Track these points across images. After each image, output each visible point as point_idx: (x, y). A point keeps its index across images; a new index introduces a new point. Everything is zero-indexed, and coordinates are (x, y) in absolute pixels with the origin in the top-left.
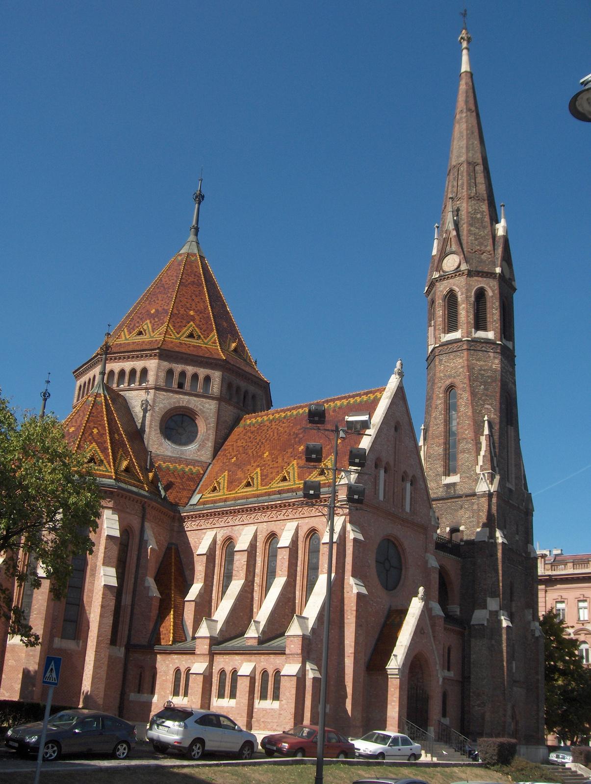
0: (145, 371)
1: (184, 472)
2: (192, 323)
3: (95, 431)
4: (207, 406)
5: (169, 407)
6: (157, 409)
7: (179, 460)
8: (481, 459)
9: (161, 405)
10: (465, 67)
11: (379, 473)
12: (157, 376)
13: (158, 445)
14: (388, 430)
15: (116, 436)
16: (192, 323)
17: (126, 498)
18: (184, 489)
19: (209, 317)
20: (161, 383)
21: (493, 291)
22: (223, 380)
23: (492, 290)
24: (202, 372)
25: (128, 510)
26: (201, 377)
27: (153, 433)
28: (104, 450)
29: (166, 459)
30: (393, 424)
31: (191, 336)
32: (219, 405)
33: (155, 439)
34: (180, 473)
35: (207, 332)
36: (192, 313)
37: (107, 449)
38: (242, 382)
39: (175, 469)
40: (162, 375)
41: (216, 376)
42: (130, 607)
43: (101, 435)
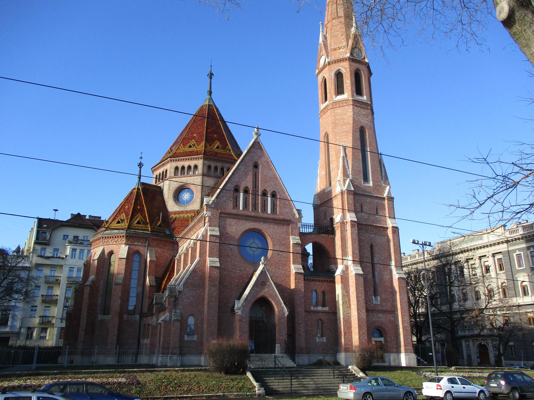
1: (184, 218)
2: (193, 140)
3: (127, 207)
4: (196, 180)
6: (171, 188)
7: (182, 212)
8: (339, 171)
9: (173, 186)
11: (240, 194)
12: (170, 172)
13: (171, 206)
14: (245, 168)
15: (139, 207)
16: (193, 140)
17: (133, 237)
19: (203, 135)
21: (345, 69)
25: (136, 243)
26: (192, 166)
27: (170, 201)
29: (175, 213)
30: (251, 164)
31: (190, 147)
34: (182, 218)
35: (199, 143)
36: (195, 135)
37: (128, 215)
40: (173, 170)
41: (200, 163)
42: (141, 295)
43: (129, 208)
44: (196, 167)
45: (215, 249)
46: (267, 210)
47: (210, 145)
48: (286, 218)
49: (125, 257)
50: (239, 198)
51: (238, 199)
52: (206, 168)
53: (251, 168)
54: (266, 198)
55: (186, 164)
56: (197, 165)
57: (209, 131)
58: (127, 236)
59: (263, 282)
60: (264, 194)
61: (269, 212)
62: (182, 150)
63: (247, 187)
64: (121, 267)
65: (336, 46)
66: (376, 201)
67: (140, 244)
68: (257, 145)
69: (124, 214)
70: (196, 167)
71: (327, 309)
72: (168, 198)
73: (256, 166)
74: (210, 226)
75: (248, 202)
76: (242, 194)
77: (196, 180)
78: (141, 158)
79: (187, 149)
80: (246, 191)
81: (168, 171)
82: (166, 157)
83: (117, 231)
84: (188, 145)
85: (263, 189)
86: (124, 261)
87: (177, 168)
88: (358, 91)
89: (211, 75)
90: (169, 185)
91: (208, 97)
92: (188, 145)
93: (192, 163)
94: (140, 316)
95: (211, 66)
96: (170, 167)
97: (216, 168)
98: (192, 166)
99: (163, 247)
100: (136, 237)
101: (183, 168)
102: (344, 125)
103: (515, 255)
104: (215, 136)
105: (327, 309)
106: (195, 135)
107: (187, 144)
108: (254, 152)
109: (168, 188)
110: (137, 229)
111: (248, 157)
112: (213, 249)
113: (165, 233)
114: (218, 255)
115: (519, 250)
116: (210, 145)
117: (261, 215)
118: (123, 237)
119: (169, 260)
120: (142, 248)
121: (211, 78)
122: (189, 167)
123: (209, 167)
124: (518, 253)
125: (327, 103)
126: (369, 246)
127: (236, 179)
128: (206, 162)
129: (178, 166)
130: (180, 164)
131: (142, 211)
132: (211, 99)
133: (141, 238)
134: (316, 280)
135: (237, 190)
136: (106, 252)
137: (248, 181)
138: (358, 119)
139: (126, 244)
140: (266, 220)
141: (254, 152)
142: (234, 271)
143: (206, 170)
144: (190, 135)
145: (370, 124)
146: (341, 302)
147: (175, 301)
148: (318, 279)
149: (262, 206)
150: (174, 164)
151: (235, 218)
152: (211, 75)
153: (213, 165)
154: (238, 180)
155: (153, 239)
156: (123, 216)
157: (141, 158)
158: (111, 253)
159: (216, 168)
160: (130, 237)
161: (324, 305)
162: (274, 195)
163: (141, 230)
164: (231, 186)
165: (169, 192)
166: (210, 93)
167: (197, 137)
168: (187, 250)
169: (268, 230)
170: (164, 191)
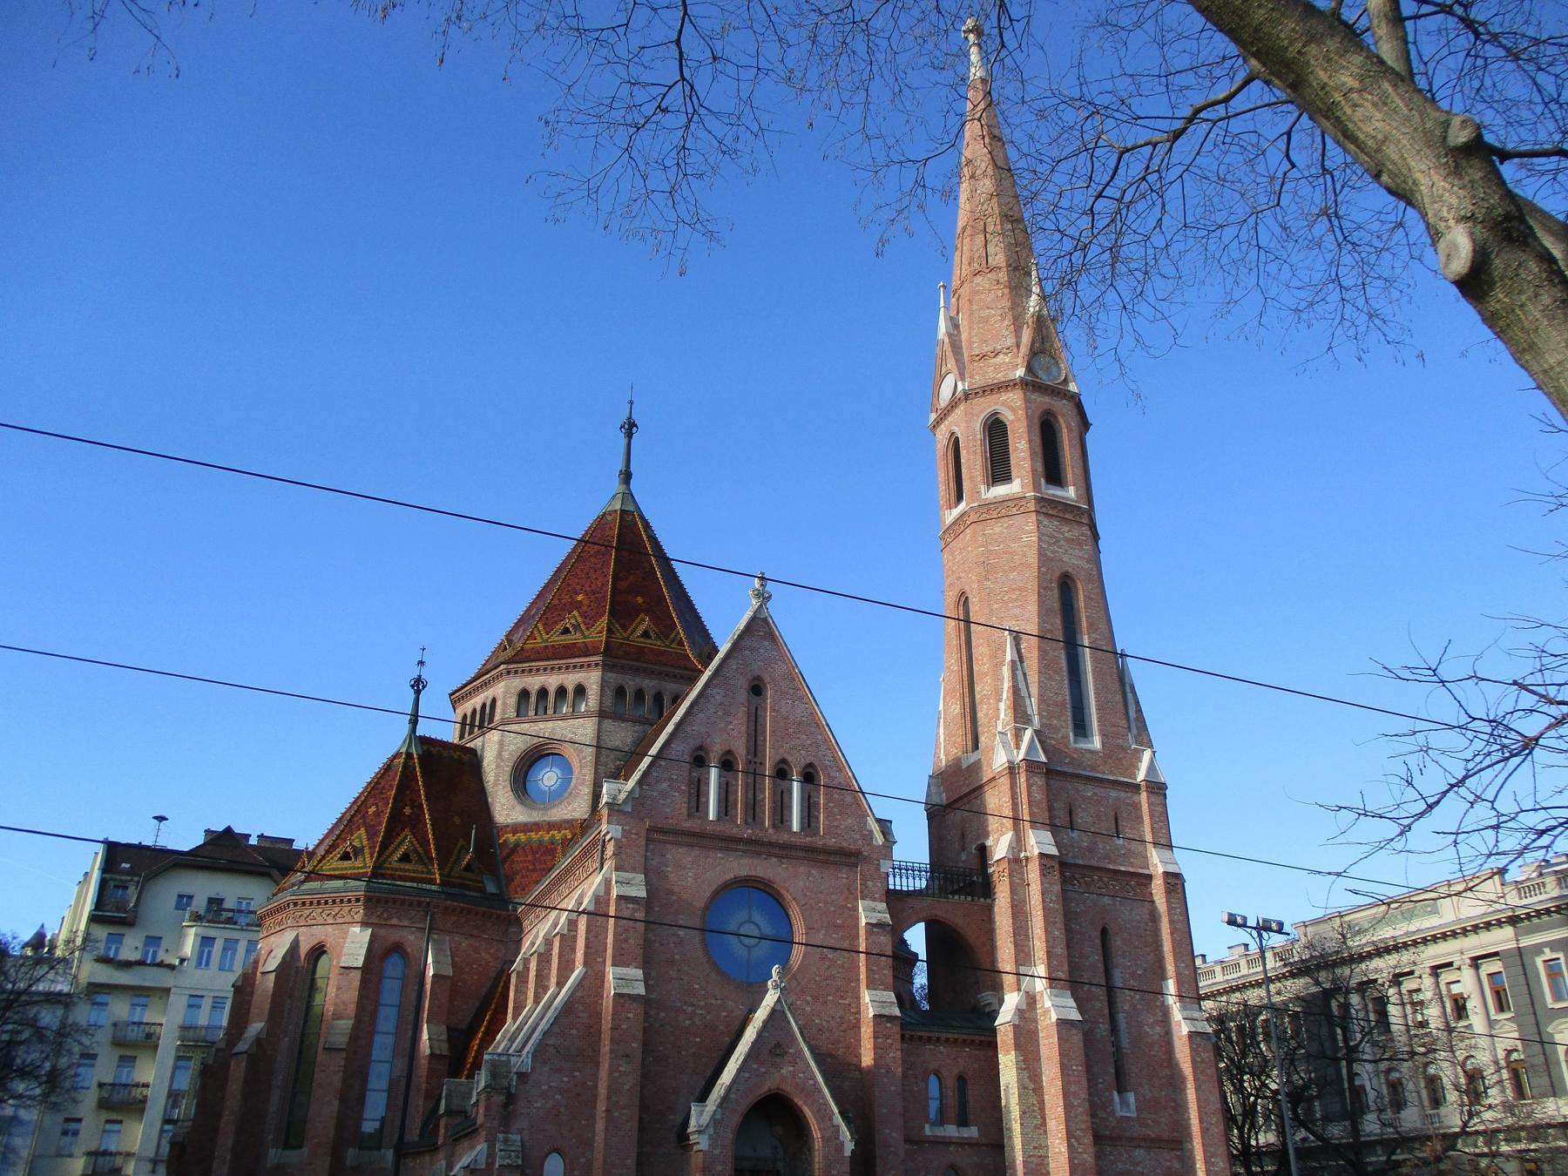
0: (494, 701)
1: (540, 842)
2: (575, 613)
3: (373, 809)
4: (581, 731)
5: (523, 747)
6: (506, 755)
7: (536, 827)
8: (1002, 706)
10: (976, 72)
12: (504, 704)
13: (505, 809)
15: (407, 811)
16: (575, 613)
17: (386, 902)
18: (534, 870)
19: (604, 597)
20: (512, 714)
21: (1014, 410)
22: (604, 684)
23: (1013, 409)
24: (570, 680)
25: (394, 921)
26: (570, 688)
27: (501, 793)
28: (371, 836)
29: (516, 828)
30: (742, 684)
31: (566, 631)
32: (600, 723)
33: (503, 801)
34: (535, 845)
35: (590, 620)
36: (580, 597)
37: (376, 834)
38: (647, 681)
39: (529, 841)
40: (513, 701)
41: (592, 679)
43: (378, 814)
44: (580, 691)
45: (631, 941)
46: (790, 821)
47: (625, 628)
48: (845, 844)
49: (360, 963)
50: (707, 785)
51: (703, 787)
52: (609, 693)
53: (743, 695)
54: (785, 784)
55: (552, 681)
56: (585, 684)
57: (622, 585)
58: (368, 900)
59: (778, 1045)
60: (782, 773)
61: (795, 827)
62: (542, 639)
63: (729, 752)
64: (345, 997)
65: (987, 348)
66: (1113, 794)
67: (406, 923)
68: (759, 629)
69: (363, 830)
70: (580, 691)
71: (972, 1132)
72: (496, 784)
73: (757, 689)
74: (617, 869)
75: (731, 798)
76: (714, 773)
77: (581, 731)
78: (421, 663)
79: (556, 639)
80: (727, 765)
81: (499, 703)
82: (494, 662)
83: (339, 883)
84: (560, 627)
85: (778, 758)
86: (356, 977)
87: (524, 694)
88: (1052, 472)
89: (630, 428)
90: (501, 743)
91: (622, 488)
92: (560, 627)
93: (570, 680)
94: (396, 1151)
95: (631, 403)
96: (503, 691)
97: (639, 695)
98: (570, 688)
99: (475, 932)
100: (395, 901)
101: (543, 693)
102: (1013, 569)
103: (1539, 961)
104: (640, 600)
105: (972, 1132)
106: (580, 597)
107: (556, 623)
108: (752, 649)
109: (496, 753)
110: (401, 878)
111: (733, 664)
112: (626, 941)
113: (482, 890)
114: (640, 959)
115: (1554, 946)
116: (625, 628)
117: (772, 835)
118: (358, 900)
119: (493, 975)
120: (412, 938)
121: (629, 435)
122: (561, 691)
123: (620, 692)
124: (1548, 954)
125: (962, 506)
126: (1098, 934)
127: (697, 727)
128: (611, 676)
129: (530, 688)
130: (534, 683)
131: (416, 823)
132: (628, 496)
133: (411, 904)
134: (938, 1039)
135: (700, 761)
136: (304, 949)
137: (735, 733)
138: (1054, 552)
139: (364, 924)
140: (786, 851)
141: (752, 649)
142: (690, 1009)
143: (609, 702)
144: (566, 599)
145: (1087, 566)
146: (1019, 1158)
147: (506, 1105)
148: (943, 1036)
149: (774, 809)
150: (517, 683)
151: (692, 846)
152: (630, 428)
153: (631, 683)
154: (703, 730)
155: (447, 908)
156: (360, 837)
157: (421, 663)
158: (319, 951)
159: (639, 695)
160: (379, 901)
161: (963, 1122)
162: (809, 777)
163: (413, 880)
164: (682, 749)
165: (498, 766)
166: (627, 476)
167: (586, 602)
168: (548, 942)
169: (793, 880)
170: (485, 764)
